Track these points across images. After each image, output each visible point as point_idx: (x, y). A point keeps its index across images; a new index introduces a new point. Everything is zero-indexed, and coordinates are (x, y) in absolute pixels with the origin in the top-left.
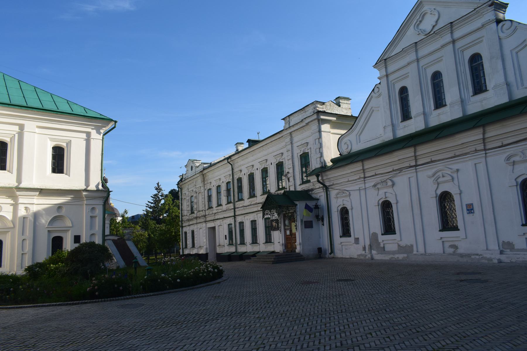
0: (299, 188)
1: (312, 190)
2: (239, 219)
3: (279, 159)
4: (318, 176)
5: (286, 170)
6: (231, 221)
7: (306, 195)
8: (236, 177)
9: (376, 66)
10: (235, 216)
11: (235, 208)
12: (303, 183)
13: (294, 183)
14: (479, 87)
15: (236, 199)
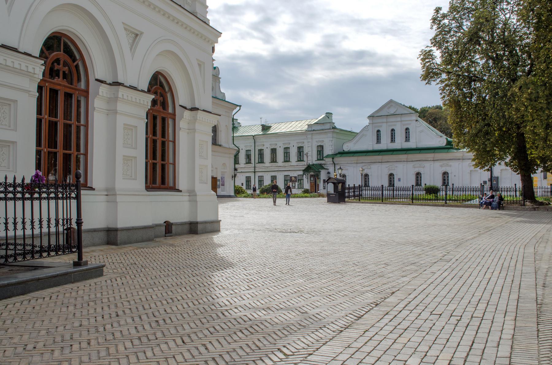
0: (315, 163)
1: (325, 164)
2: (260, 174)
3: (300, 145)
4: (333, 159)
5: (306, 150)
6: (252, 175)
7: (321, 167)
8: (257, 148)
9: (369, 117)
10: (255, 172)
11: (255, 167)
12: (318, 160)
13: (312, 158)
14: (407, 139)
15: (257, 161)
